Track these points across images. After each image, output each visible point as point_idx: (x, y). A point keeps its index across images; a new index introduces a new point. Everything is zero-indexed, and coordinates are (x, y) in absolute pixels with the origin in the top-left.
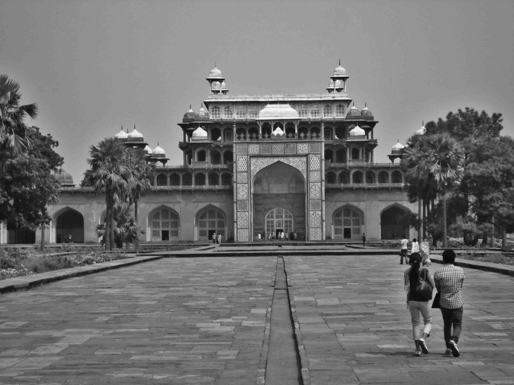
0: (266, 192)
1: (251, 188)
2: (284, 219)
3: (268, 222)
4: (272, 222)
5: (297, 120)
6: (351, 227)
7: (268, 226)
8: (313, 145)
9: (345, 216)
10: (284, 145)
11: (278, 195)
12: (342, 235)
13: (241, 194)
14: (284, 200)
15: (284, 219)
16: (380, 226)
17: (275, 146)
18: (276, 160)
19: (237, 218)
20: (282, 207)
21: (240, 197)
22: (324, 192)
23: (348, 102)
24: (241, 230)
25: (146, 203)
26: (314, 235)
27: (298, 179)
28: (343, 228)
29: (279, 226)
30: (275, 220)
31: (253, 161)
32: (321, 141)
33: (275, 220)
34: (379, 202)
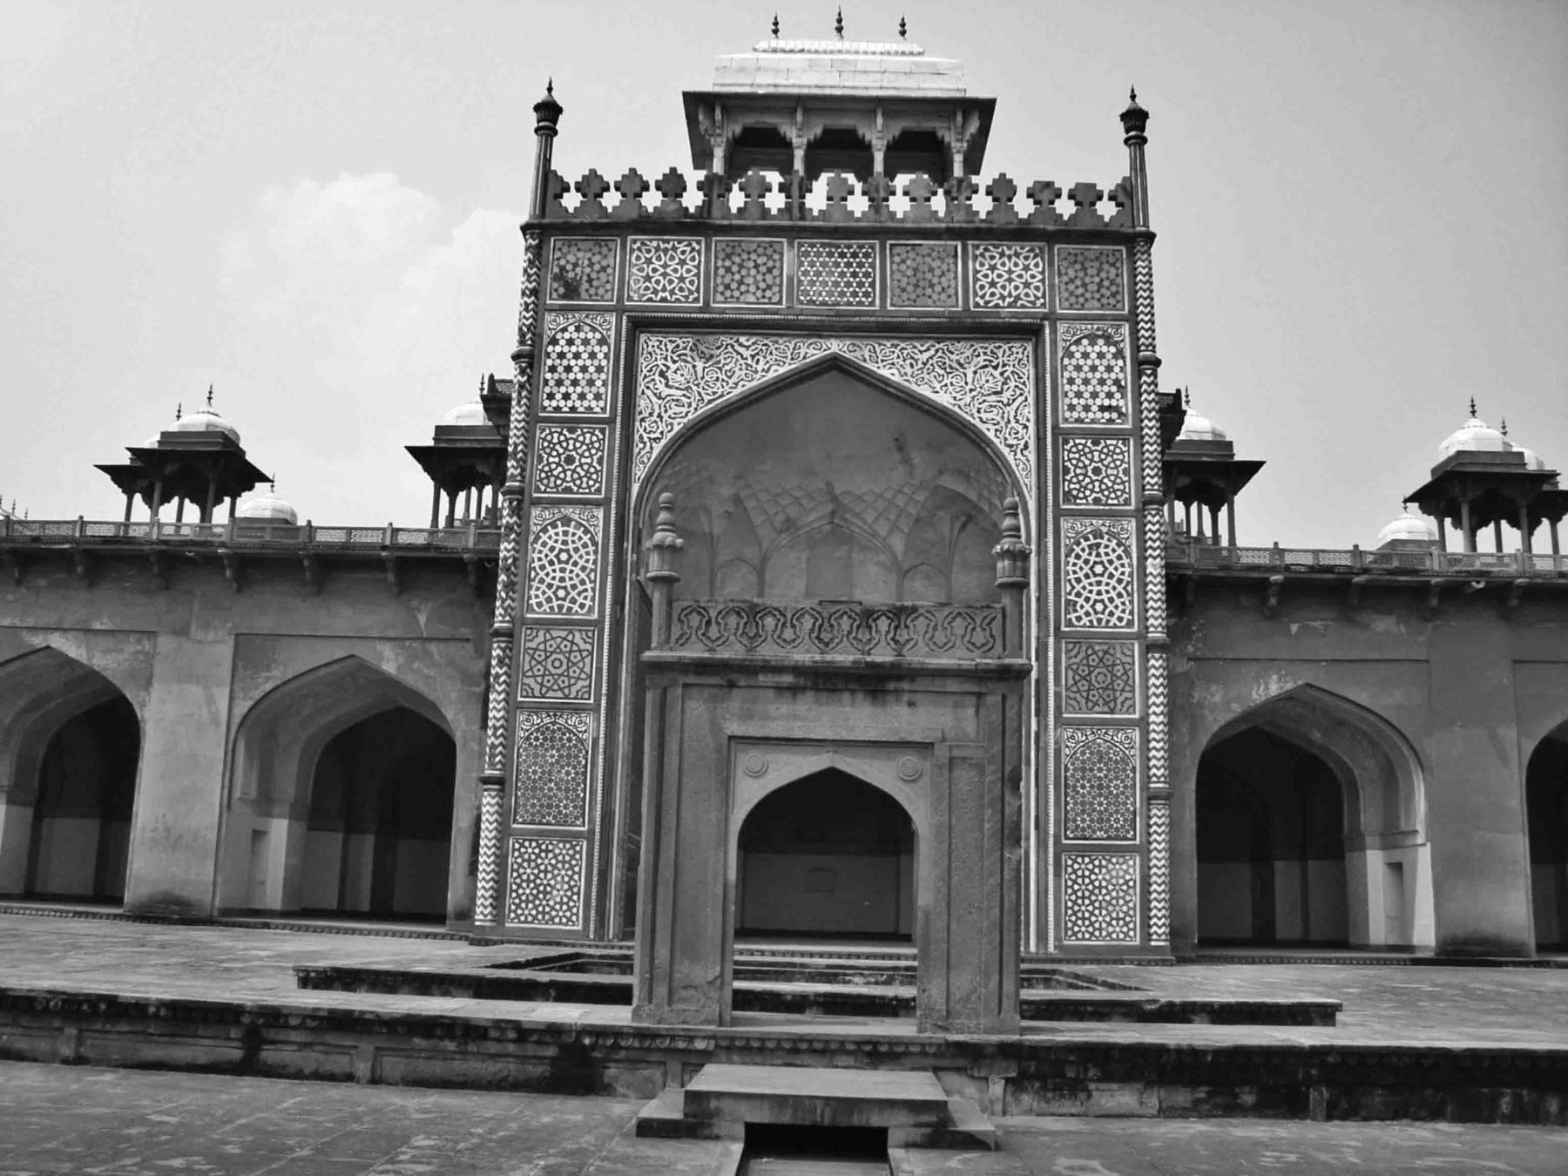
18: (813, 351)
22: (1156, 589)
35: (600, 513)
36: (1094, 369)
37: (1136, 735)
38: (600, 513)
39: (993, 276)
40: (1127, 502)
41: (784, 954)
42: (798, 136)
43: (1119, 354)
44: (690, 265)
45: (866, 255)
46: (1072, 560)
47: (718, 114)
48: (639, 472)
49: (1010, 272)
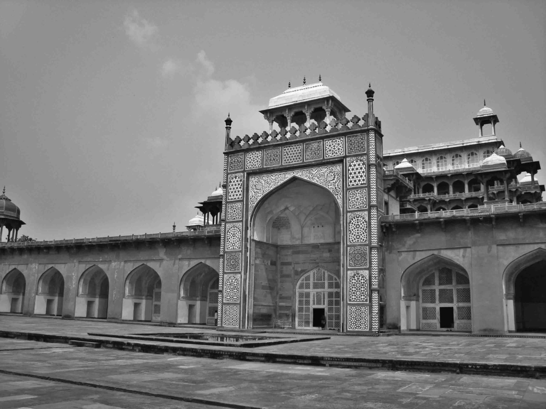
0: (298, 242)
1: (247, 228)
2: (327, 290)
3: (301, 295)
4: (308, 295)
6: (455, 305)
7: (301, 302)
8: (353, 139)
10: (301, 147)
11: (316, 247)
12: (436, 322)
13: (231, 240)
14: (326, 255)
15: (327, 290)
16: (511, 303)
17: (287, 149)
18: (289, 176)
19: (223, 285)
20: (323, 267)
21: (229, 247)
22: (375, 230)
23: (498, 144)
25: (126, 262)
26: (353, 320)
27: (328, 208)
28: (438, 306)
29: (319, 303)
30: (312, 291)
31: (253, 180)
33: (312, 291)
34: (500, 248)
35: (241, 224)
36: (357, 169)
37: (367, 272)
38: (241, 224)
39: (330, 148)
40: (366, 207)
41: (265, 332)
43: (363, 164)
44: (259, 157)
45: (299, 148)
46: (351, 225)
47: (268, 115)
48: (250, 213)
49: (334, 146)
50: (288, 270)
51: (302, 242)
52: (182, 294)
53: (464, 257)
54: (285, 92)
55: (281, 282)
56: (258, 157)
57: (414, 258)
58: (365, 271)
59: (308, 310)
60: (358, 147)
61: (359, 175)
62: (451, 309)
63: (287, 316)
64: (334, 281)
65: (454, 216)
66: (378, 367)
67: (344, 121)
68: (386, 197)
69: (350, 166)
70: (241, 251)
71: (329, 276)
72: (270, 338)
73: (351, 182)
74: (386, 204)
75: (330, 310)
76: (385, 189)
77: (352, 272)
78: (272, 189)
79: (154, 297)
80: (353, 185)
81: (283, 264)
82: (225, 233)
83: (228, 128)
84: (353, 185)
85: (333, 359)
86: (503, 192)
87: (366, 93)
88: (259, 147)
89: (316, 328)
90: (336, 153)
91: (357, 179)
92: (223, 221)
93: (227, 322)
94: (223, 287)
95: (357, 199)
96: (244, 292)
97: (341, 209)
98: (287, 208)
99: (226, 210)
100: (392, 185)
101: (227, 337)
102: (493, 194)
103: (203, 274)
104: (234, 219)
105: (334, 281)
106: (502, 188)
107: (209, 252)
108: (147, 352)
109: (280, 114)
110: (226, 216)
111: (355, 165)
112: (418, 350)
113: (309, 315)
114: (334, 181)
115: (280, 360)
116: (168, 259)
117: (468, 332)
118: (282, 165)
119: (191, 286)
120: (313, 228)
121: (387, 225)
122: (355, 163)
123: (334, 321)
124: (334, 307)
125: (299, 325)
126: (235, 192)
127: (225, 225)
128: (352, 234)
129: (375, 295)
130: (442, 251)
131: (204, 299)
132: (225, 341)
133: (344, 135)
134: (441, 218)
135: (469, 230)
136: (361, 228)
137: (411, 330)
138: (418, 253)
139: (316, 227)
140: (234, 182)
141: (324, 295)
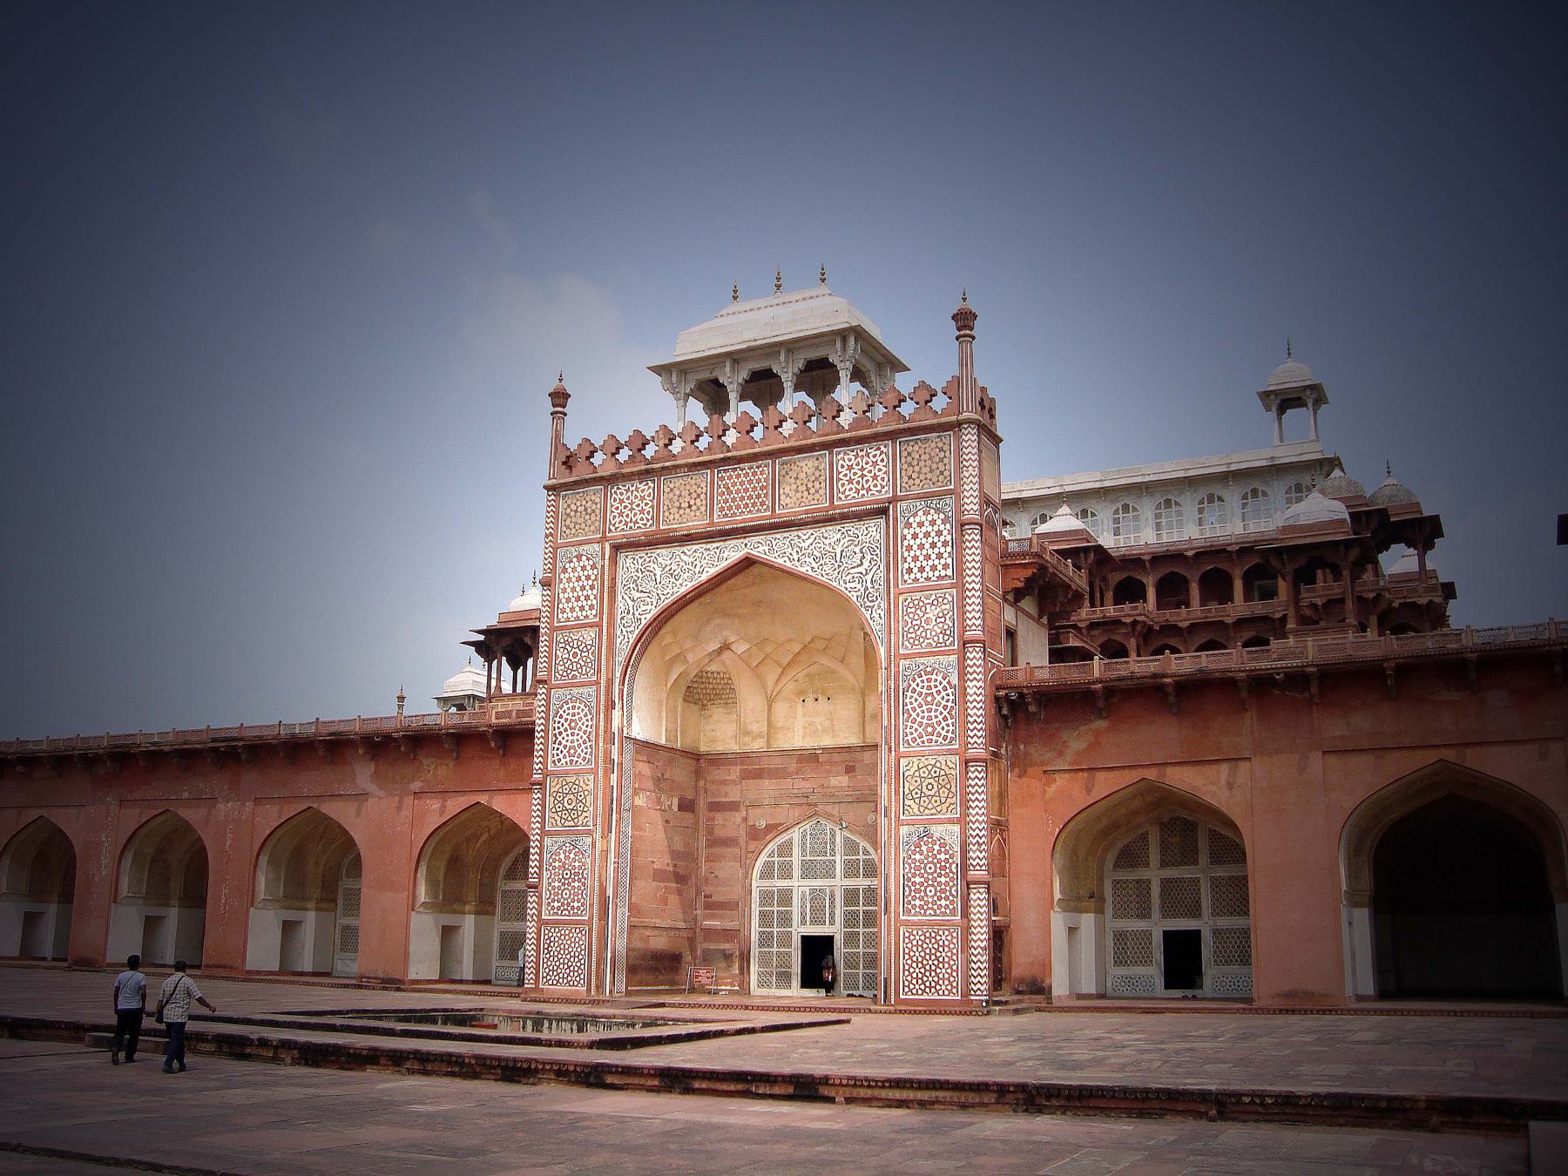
0: (757, 745)
1: (611, 705)
3: (766, 897)
4: (786, 897)
5: (843, 334)
6: (1204, 925)
7: (765, 918)
9: (1164, 864)
11: (809, 758)
12: (1153, 972)
13: (565, 739)
14: (840, 781)
15: (840, 882)
16: (1363, 916)
18: (733, 552)
20: (829, 816)
22: (978, 710)
24: (555, 933)
28: (1157, 927)
32: (959, 424)
33: (799, 886)
34: (1332, 759)
35: (592, 690)
36: (927, 535)
37: (957, 828)
40: (952, 644)
41: (662, 1005)
42: (733, 381)
47: (674, 379)
48: (621, 658)
49: (863, 469)
50: (730, 824)
51: (769, 745)
52: (422, 894)
53: (1230, 786)
54: (724, 312)
55: (708, 860)
56: (643, 498)
57: (1089, 791)
58: (950, 827)
59: (786, 939)
60: (931, 471)
61: (933, 553)
62: (1195, 936)
63: (727, 957)
64: (861, 857)
65: (1200, 671)
66: (983, 1105)
67: (891, 399)
68: (1009, 615)
69: (909, 525)
70: (595, 772)
71: (846, 839)
72: (676, 1021)
73: (910, 571)
74: (1011, 634)
75: (851, 939)
76: (1005, 593)
77: (912, 829)
78: (683, 590)
79: (340, 901)
80: (916, 580)
81: (716, 807)
82: (547, 719)
83: (558, 416)
84: (916, 580)
85: (856, 1082)
86: (1342, 601)
87: (954, 317)
88: (647, 471)
89: (810, 993)
90: (869, 489)
91: (927, 565)
92: (545, 682)
93: (553, 977)
94: (540, 876)
95: (928, 621)
96: (603, 890)
97: (882, 650)
98: (726, 647)
99: (550, 653)
100: (1028, 580)
101: (551, 1018)
102: (1313, 606)
103: (485, 836)
104: (574, 677)
105: (861, 857)
106: (1336, 590)
107: (502, 773)
108: (316, 1064)
109: (706, 375)
110: (549, 669)
111: (921, 525)
112: (1100, 1054)
113: (789, 954)
114: (861, 569)
115: (704, 1085)
116: (382, 793)
117: (1244, 1002)
118: (712, 523)
119: (446, 874)
120: (800, 706)
121: (1013, 696)
122: (921, 517)
123: (861, 971)
124: (861, 930)
125: (761, 985)
126: (578, 599)
127: (548, 695)
128: (914, 721)
129: (979, 898)
130: (1169, 770)
131: (485, 907)
132: (545, 1030)
133: (891, 436)
134: (1164, 676)
135: (1245, 710)
136: (938, 704)
137: (1080, 997)
138: (1100, 775)
139: (810, 700)
140: (574, 570)
141: (832, 896)
